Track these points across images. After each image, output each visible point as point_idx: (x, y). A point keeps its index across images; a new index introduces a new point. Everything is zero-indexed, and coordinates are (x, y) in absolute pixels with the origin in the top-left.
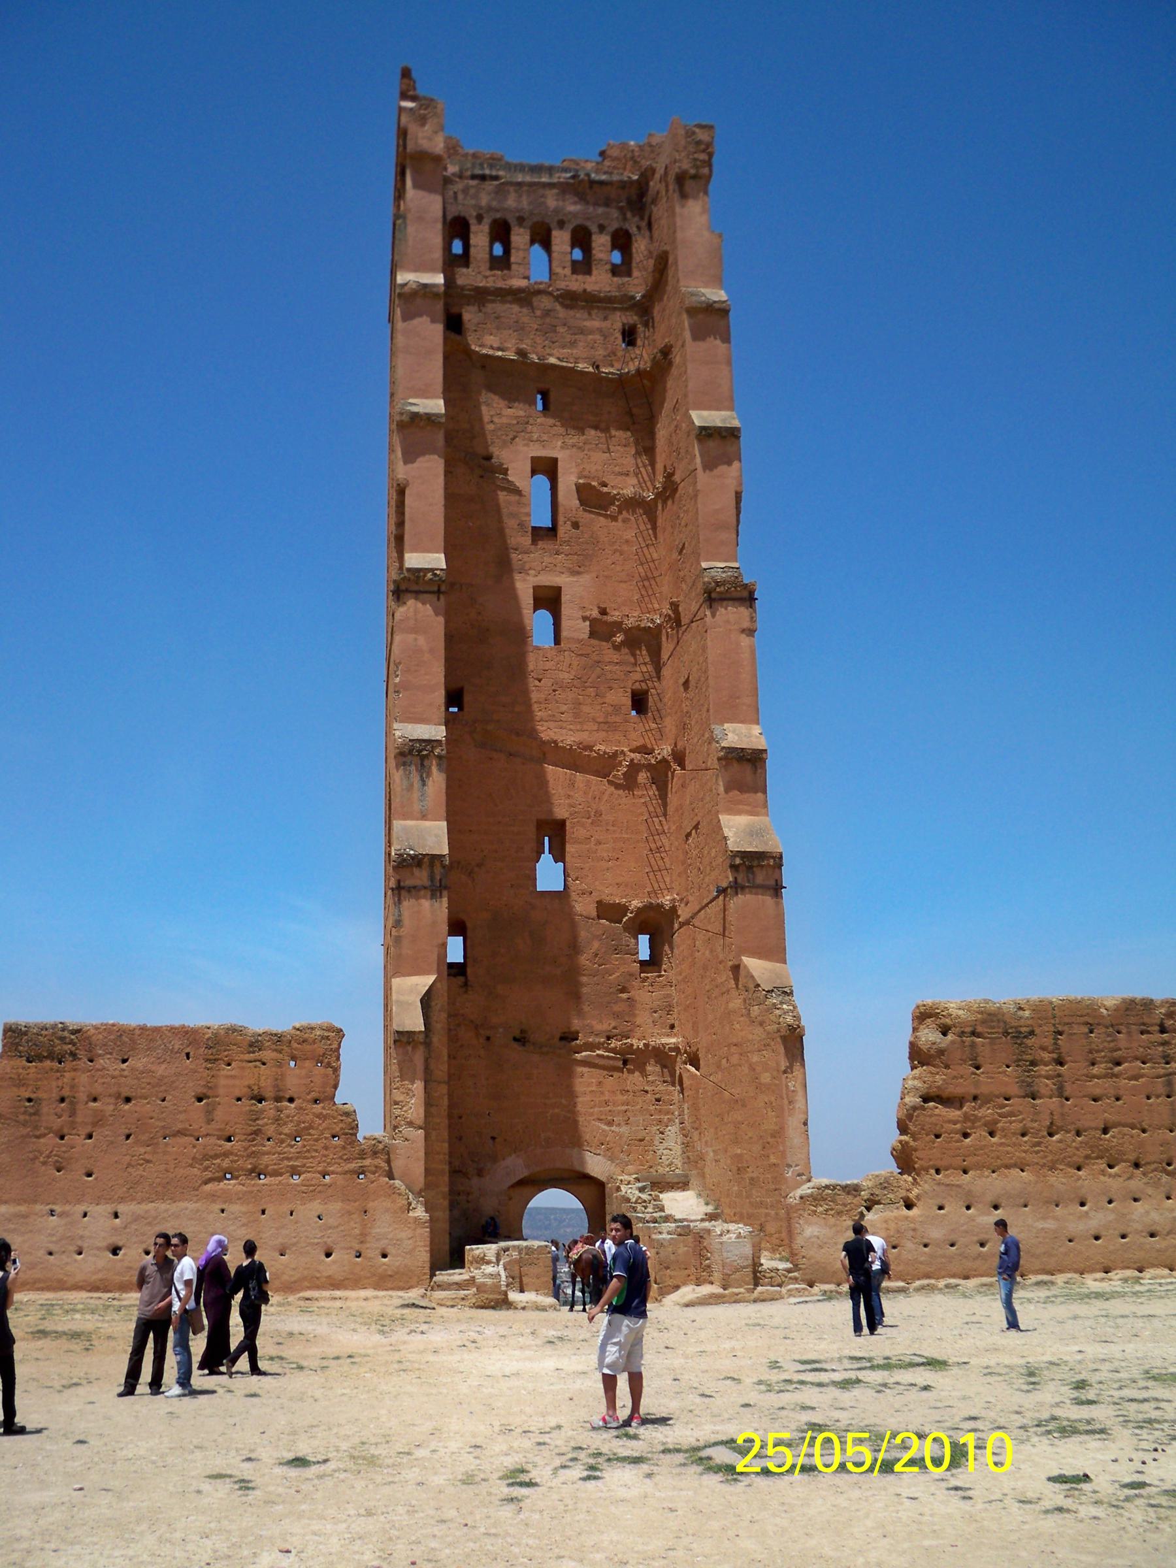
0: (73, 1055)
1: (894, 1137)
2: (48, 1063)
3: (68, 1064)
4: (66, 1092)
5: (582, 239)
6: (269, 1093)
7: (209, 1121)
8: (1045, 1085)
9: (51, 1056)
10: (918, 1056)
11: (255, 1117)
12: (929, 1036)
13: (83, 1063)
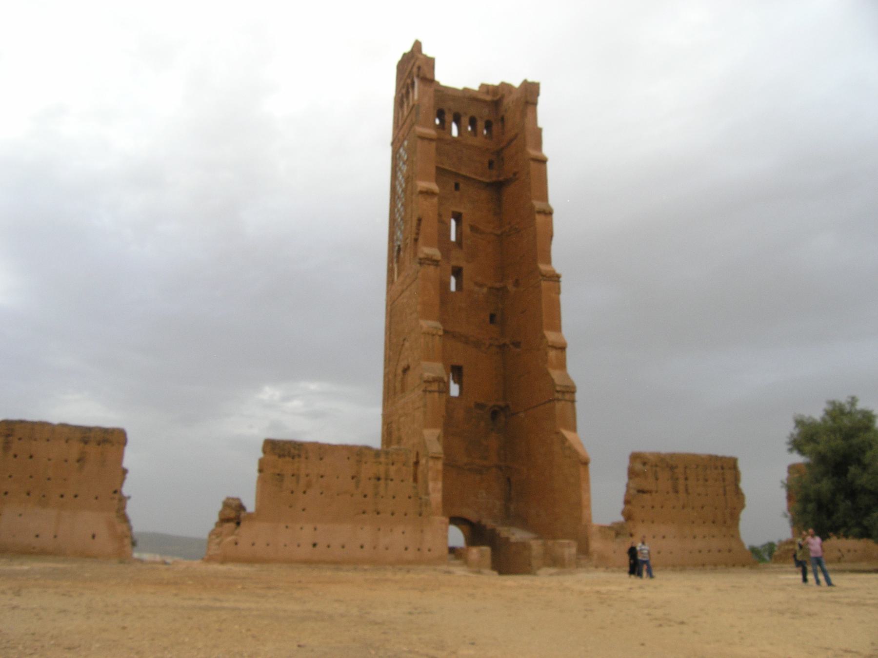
0: (299, 456)
1: (621, 506)
2: (288, 459)
3: (297, 459)
5: (473, 122)
6: (383, 476)
7: (357, 487)
8: (681, 488)
9: (289, 455)
10: (632, 473)
11: (376, 487)
12: (638, 466)
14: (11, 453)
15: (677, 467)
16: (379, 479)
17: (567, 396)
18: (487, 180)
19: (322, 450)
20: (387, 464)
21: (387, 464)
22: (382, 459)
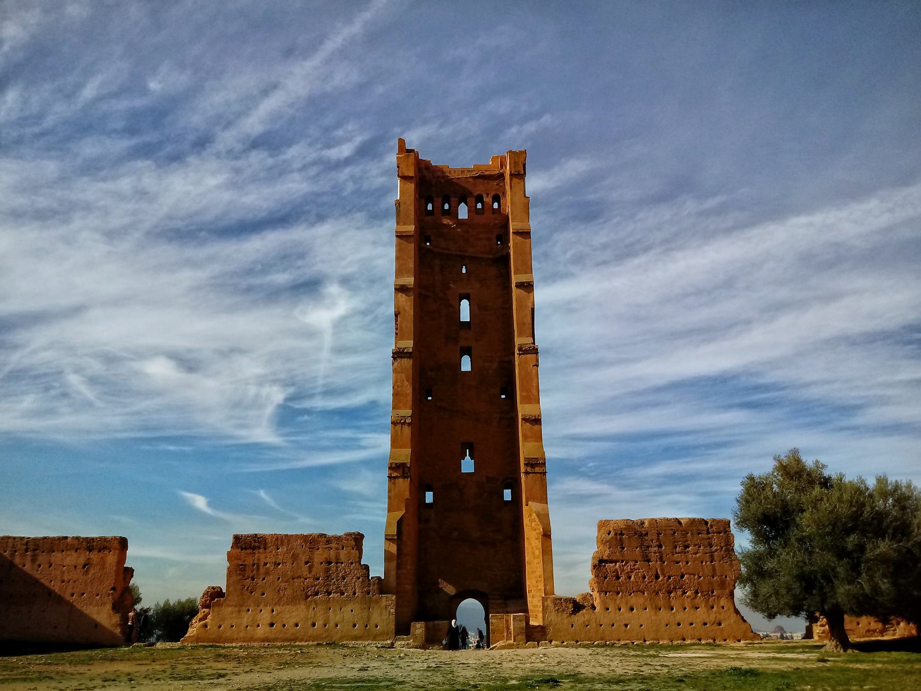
4: (256, 562)
6: (334, 560)
7: (310, 572)
8: (653, 557)
13: (262, 550)
14: (37, 563)
15: (647, 534)
16: (330, 563)
17: (537, 469)
18: (491, 256)
19: (281, 540)
20: (338, 549)
21: (338, 549)
22: (334, 545)
